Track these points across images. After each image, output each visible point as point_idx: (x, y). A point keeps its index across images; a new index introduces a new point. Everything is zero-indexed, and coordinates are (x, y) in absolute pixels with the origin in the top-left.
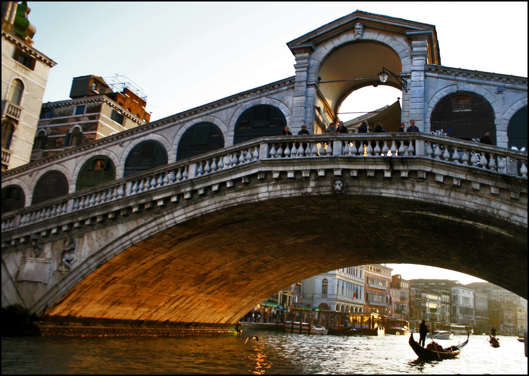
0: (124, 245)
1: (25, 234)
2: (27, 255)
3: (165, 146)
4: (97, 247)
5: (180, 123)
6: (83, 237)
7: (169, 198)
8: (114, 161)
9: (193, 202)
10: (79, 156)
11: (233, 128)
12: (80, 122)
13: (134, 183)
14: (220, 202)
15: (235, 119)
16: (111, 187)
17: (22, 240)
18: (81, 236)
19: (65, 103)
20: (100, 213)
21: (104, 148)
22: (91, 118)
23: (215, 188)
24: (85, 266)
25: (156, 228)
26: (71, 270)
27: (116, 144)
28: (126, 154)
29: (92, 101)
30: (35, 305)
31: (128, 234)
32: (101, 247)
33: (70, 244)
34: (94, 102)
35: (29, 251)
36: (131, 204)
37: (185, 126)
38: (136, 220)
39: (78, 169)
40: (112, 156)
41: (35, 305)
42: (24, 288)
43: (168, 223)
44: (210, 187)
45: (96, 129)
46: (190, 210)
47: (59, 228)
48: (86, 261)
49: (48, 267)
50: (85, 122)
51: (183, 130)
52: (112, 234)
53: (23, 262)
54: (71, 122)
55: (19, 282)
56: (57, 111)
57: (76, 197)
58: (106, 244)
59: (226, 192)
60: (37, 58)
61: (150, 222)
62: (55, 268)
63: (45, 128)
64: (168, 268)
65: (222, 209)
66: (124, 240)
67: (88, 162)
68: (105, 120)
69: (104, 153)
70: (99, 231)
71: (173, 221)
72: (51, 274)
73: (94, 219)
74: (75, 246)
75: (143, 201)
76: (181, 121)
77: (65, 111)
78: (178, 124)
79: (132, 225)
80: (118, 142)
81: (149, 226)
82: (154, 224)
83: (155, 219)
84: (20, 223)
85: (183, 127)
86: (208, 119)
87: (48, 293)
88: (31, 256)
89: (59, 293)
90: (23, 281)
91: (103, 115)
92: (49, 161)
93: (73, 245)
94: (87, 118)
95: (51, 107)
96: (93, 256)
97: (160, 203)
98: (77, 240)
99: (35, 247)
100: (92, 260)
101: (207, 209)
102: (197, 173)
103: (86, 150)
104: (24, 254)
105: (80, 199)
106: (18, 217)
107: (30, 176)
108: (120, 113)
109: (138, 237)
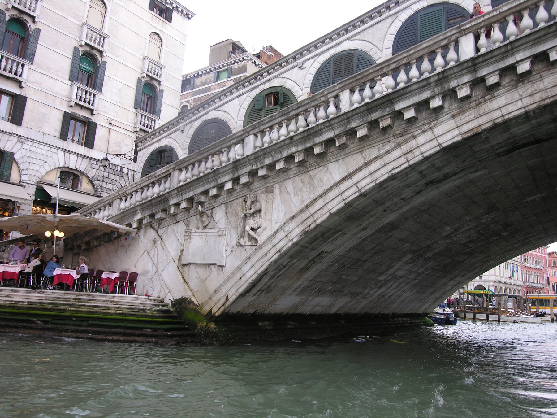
0: (344, 196)
1: (186, 196)
2: (192, 226)
3: (371, 53)
4: (297, 204)
5: (390, 16)
6: (272, 191)
7: (427, 102)
8: (293, 91)
9: (473, 104)
10: (243, 94)
13: (352, 91)
14: (532, 95)
16: (313, 104)
17: (184, 205)
18: (269, 190)
19: (206, 71)
20: (300, 148)
21: (276, 77)
24: (281, 235)
25: (403, 160)
26: (259, 243)
27: (293, 68)
28: (311, 77)
29: (235, 62)
30: (210, 298)
31: (350, 176)
32: (306, 203)
33: (253, 203)
34: (238, 63)
35: (194, 221)
36: (354, 124)
37: (399, 18)
38: (361, 152)
39: (243, 111)
40: (289, 85)
41: (210, 298)
42: (193, 274)
43: (423, 149)
44: (512, 68)
46: (467, 119)
47: (236, 180)
48: (282, 228)
52: (321, 180)
53: (186, 238)
54: (215, 89)
55: (184, 265)
56: (198, 81)
57: (257, 130)
58: (312, 197)
59: (544, 74)
60: (173, 7)
61: (388, 152)
62: (234, 242)
63: (187, 102)
64: (391, 236)
65: (538, 108)
66: (343, 187)
67: (256, 100)
69: (276, 83)
70: (297, 178)
71: (435, 143)
72: (229, 251)
73: (290, 158)
74: (261, 205)
76: (392, 12)
77: (206, 80)
78: (387, 18)
79: (354, 161)
80: (295, 64)
81: (387, 158)
82: (397, 153)
83: (399, 145)
84: (180, 182)
85: (396, 21)
87: (228, 280)
88: (198, 228)
89: (244, 279)
90: (189, 264)
92: (204, 109)
93: (258, 204)
94: (232, 81)
95: (192, 78)
96: (293, 217)
97: (409, 114)
98: (262, 197)
99: (201, 214)
100: (292, 225)
101: (504, 111)
103: (250, 84)
104: (187, 225)
105: (263, 132)
106: (176, 173)
107: (182, 131)
109: (368, 180)
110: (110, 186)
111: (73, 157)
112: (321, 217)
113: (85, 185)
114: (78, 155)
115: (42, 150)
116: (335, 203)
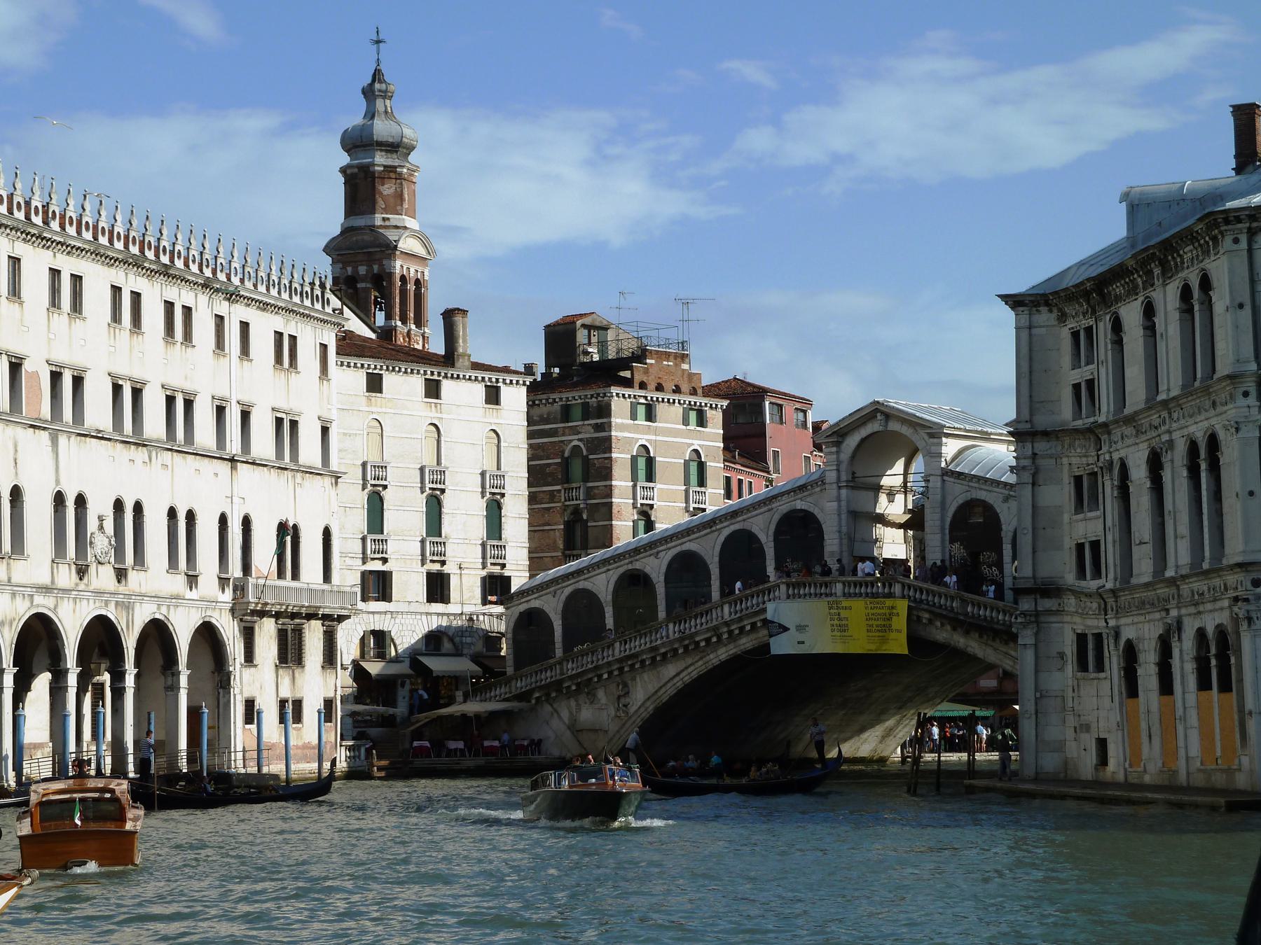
4: (651, 689)
11: (771, 538)
12: (580, 436)
15: (773, 527)
18: (634, 679)
22: (598, 428)
23: (748, 628)
24: (642, 710)
36: (676, 646)
40: (648, 570)
45: (610, 450)
47: (610, 673)
49: (605, 713)
50: (588, 436)
51: (722, 538)
54: (563, 435)
68: (623, 428)
69: (637, 565)
73: (643, 662)
75: (687, 642)
77: (549, 414)
79: (681, 665)
82: (700, 663)
86: (746, 526)
91: (615, 420)
99: (588, 694)
100: (648, 703)
102: (730, 614)
108: (642, 401)
110: (469, 640)
111: (435, 617)
112: (665, 698)
113: (447, 646)
114: (438, 614)
115: (409, 620)
116: (670, 691)
